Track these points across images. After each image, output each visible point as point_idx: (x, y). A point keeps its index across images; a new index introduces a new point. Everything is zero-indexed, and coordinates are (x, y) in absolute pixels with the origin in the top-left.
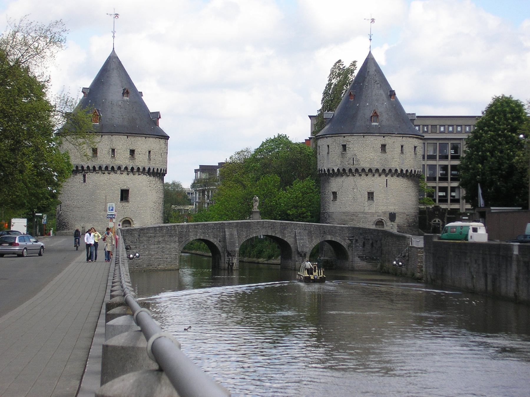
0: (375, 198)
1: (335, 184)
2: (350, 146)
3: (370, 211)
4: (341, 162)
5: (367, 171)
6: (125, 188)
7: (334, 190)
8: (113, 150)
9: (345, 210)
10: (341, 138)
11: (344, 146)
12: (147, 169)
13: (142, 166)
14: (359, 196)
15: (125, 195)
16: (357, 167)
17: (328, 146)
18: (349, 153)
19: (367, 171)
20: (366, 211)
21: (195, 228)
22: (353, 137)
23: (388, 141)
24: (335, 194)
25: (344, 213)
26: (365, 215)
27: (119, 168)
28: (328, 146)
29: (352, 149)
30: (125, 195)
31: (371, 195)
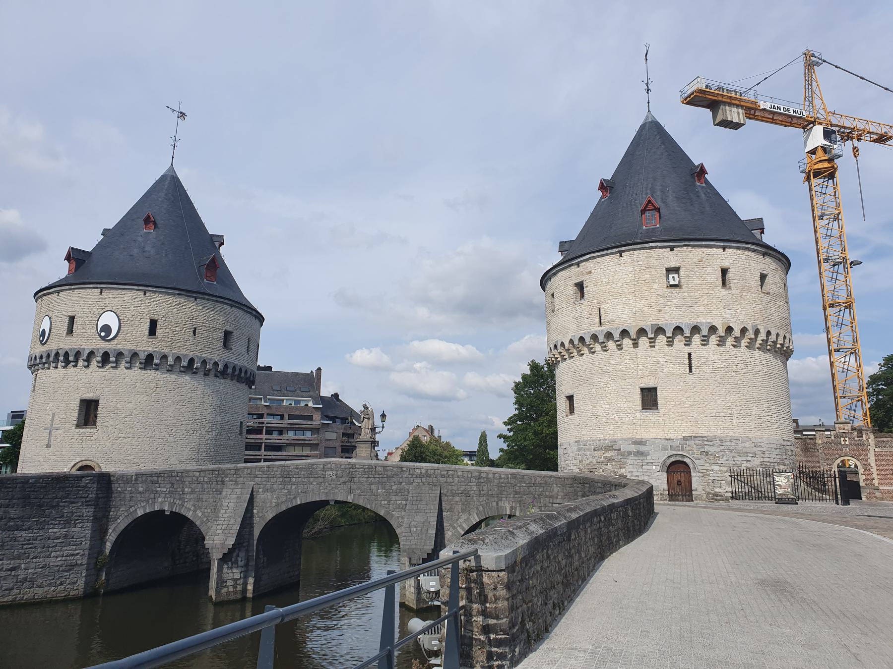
0: (660, 401)
5: (633, 334)
6: (89, 396)
8: (72, 319)
10: (574, 269)
12: (143, 356)
13: (130, 351)
15: (88, 412)
16: (605, 328)
19: (633, 334)
23: (683, 256)
24: (570, 398)
27: (78, 354)
30: (88, 412)
31: (649, 398)
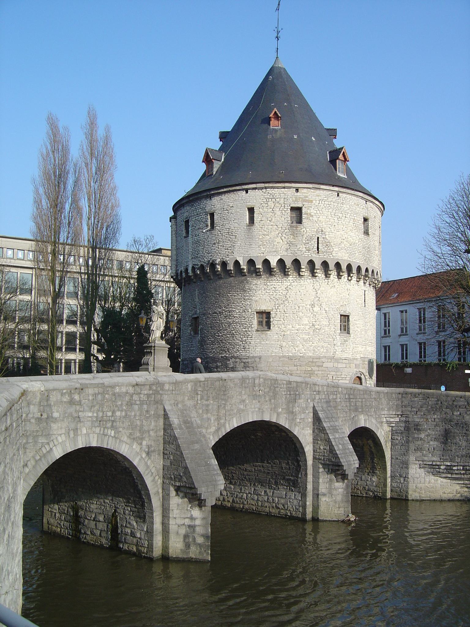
1: (263, 293)
2: (312, 211)
3: (345, 356)
4: (290, 244)
7: (264, 307)
9: (291, 351)
11: (297, 211)
14: (325, 322)
17: (251, 210)
18: (308, 227)
20: (339, 355)
21: (72, 402)
22: (318, 192)
25: (290, 358)
26: (336, 365)
28: (251, 210)
29: (315, 218)
